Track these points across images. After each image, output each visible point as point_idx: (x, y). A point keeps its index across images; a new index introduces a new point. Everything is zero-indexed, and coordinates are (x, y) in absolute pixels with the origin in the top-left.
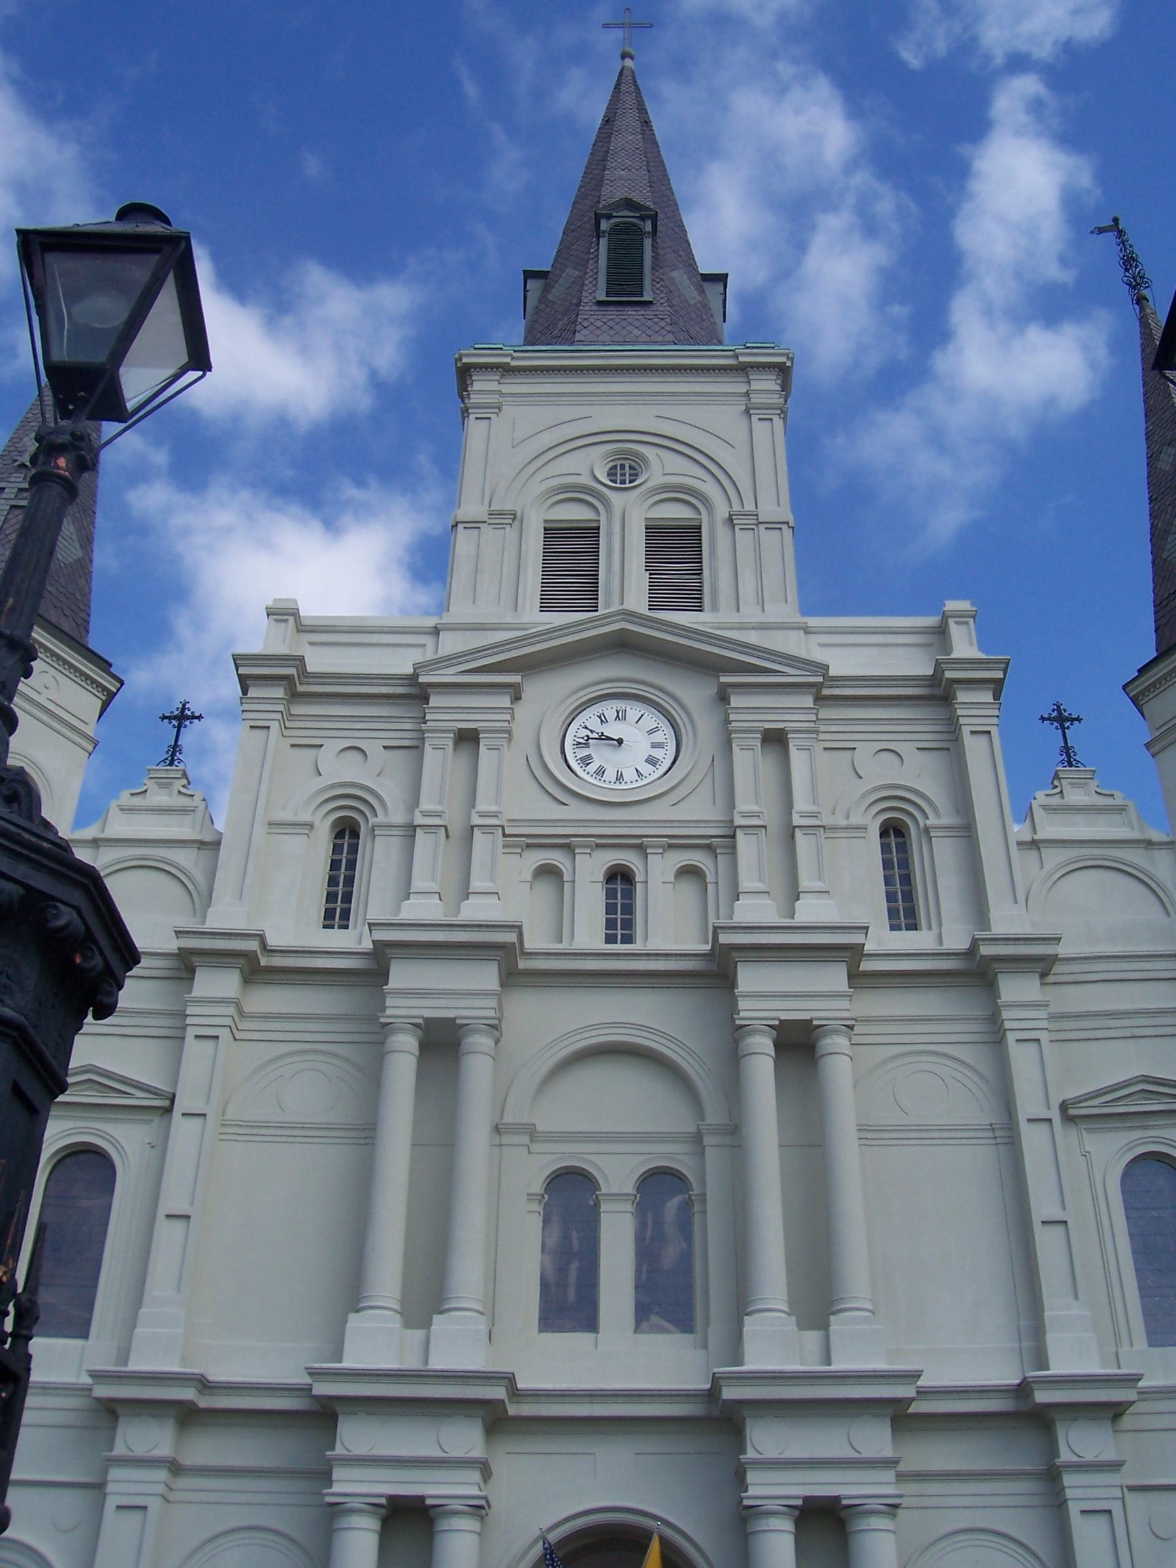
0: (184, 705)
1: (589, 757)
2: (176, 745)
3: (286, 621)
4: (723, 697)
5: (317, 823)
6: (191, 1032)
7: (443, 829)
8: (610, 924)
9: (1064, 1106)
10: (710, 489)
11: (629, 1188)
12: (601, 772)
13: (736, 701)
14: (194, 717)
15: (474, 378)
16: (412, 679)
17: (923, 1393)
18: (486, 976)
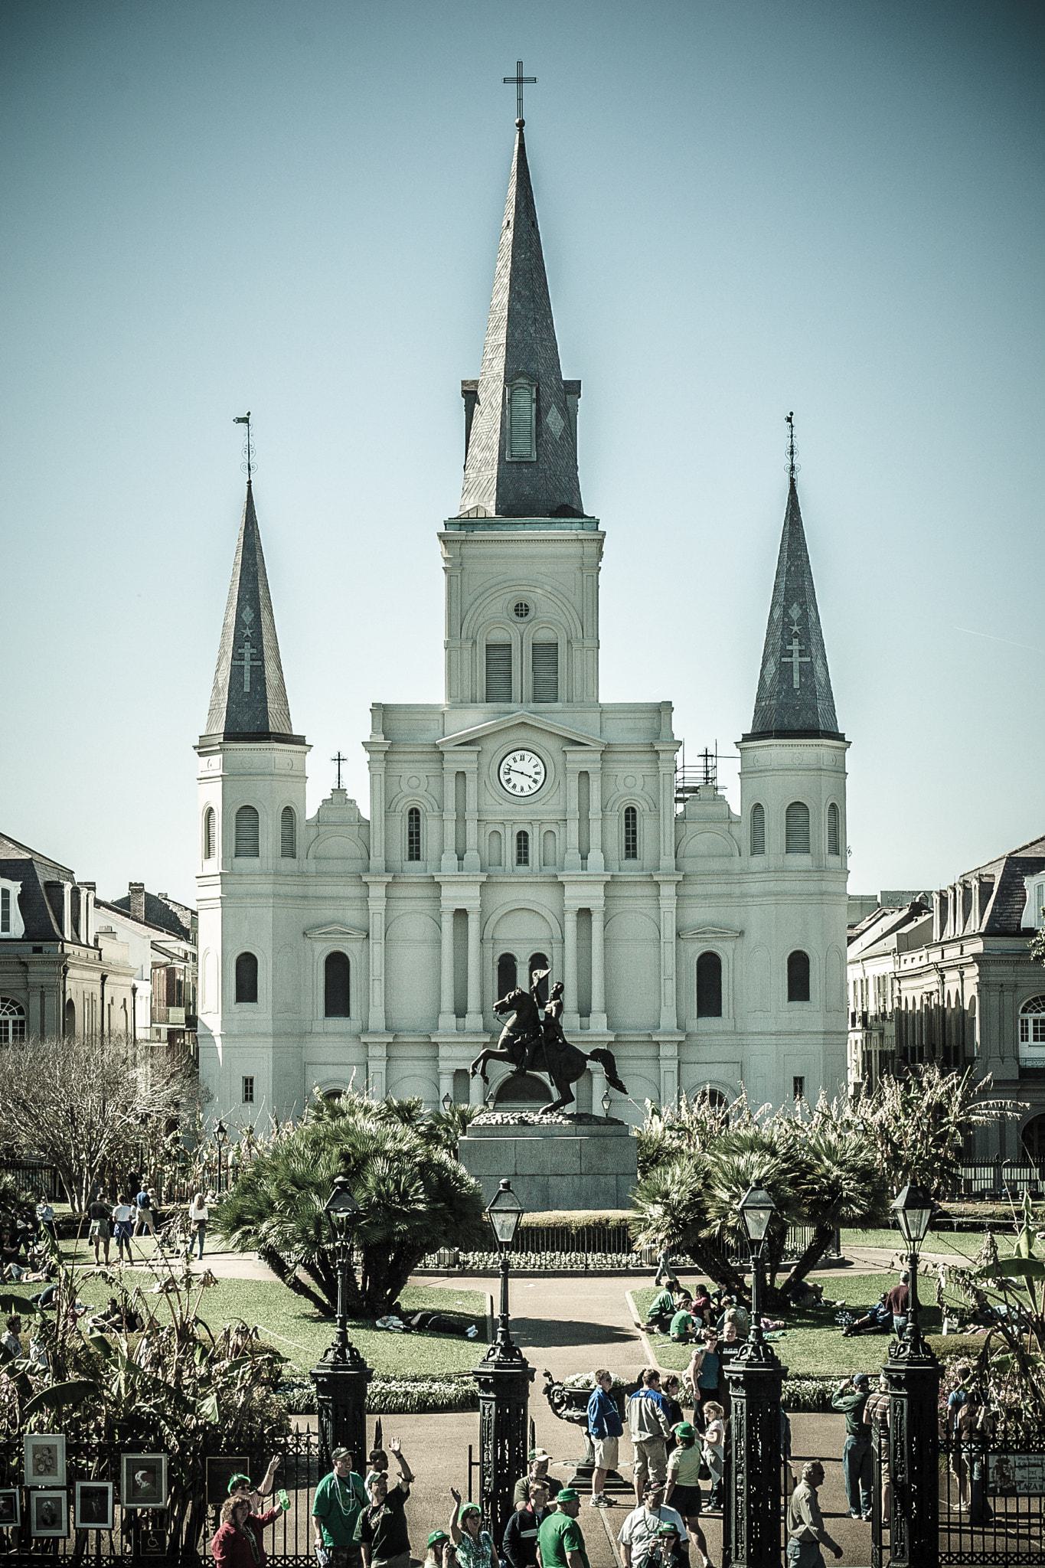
1: (510, 779)
8: (519, 854)
9: (678, 935)
12: (514, 786)
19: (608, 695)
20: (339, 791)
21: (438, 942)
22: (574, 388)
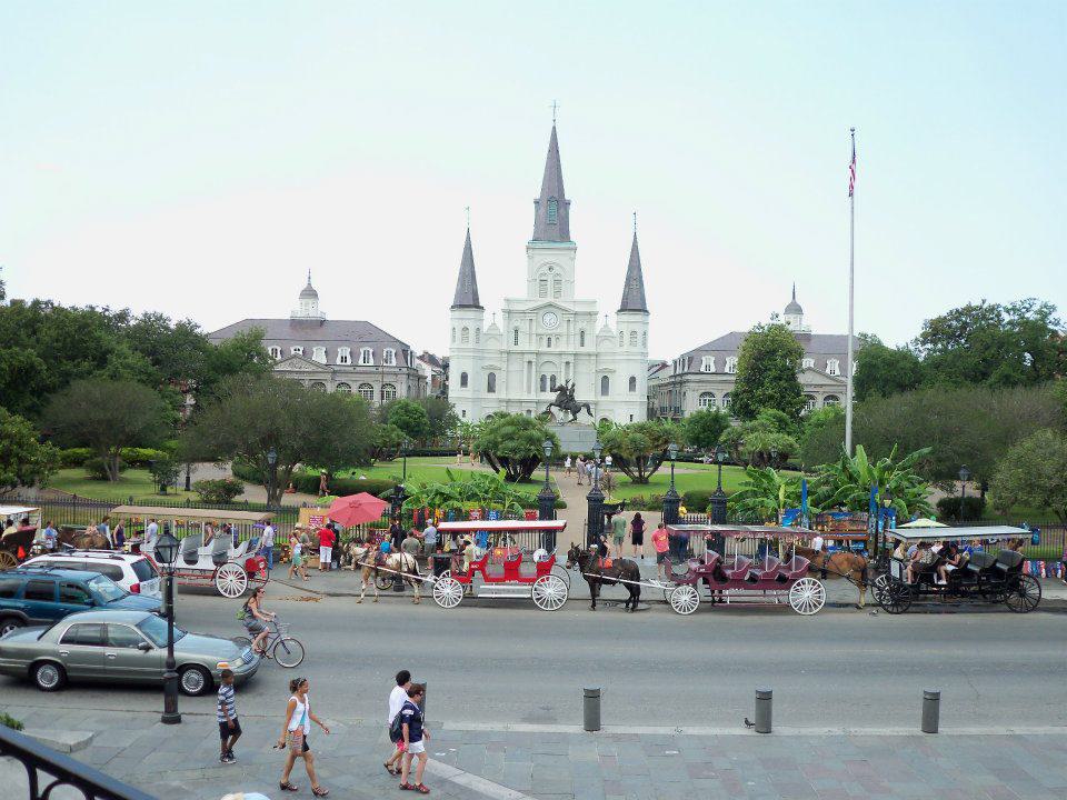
19: (577, 297)
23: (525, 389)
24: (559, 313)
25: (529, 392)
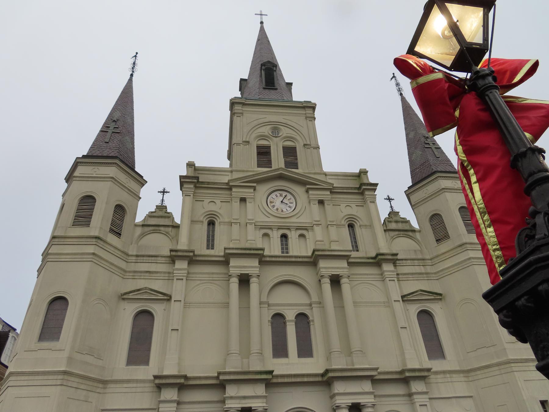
0: (164, 189)
2: (163, 200)
3: (192, 167)
4: (307, 191)
5: (204, 220)
6: (175, 278)
7: (239, 223)
8: (282, 249)
9: (403, 297)
10: (298, 138)
11: (294, 319)
12: (277, 209)
13: (310, 192)
14: (161, 192)
15: (235, 106)
16: (227, 184)
17: (380, 373)
18: (255, 262)
20: (162, 208)
21: (227, 305)
22: (290, 84)
23: (235, 346)
24: (299, 190)
25: (246, 352)
